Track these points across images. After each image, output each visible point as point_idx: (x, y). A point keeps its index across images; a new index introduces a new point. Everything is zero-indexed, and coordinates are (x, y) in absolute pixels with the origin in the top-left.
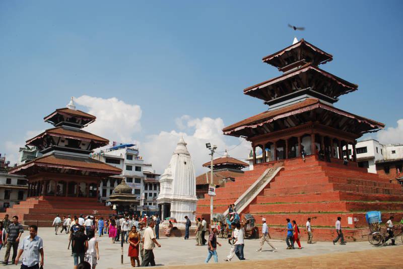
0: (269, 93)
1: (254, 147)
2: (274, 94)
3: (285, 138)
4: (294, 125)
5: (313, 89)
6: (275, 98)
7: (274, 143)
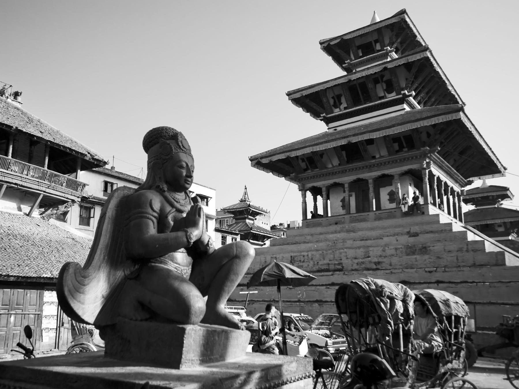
1: (303, 190)
2: (341, 104)
3: (370, 175)
6: (341, 111)
7: (346, 186)
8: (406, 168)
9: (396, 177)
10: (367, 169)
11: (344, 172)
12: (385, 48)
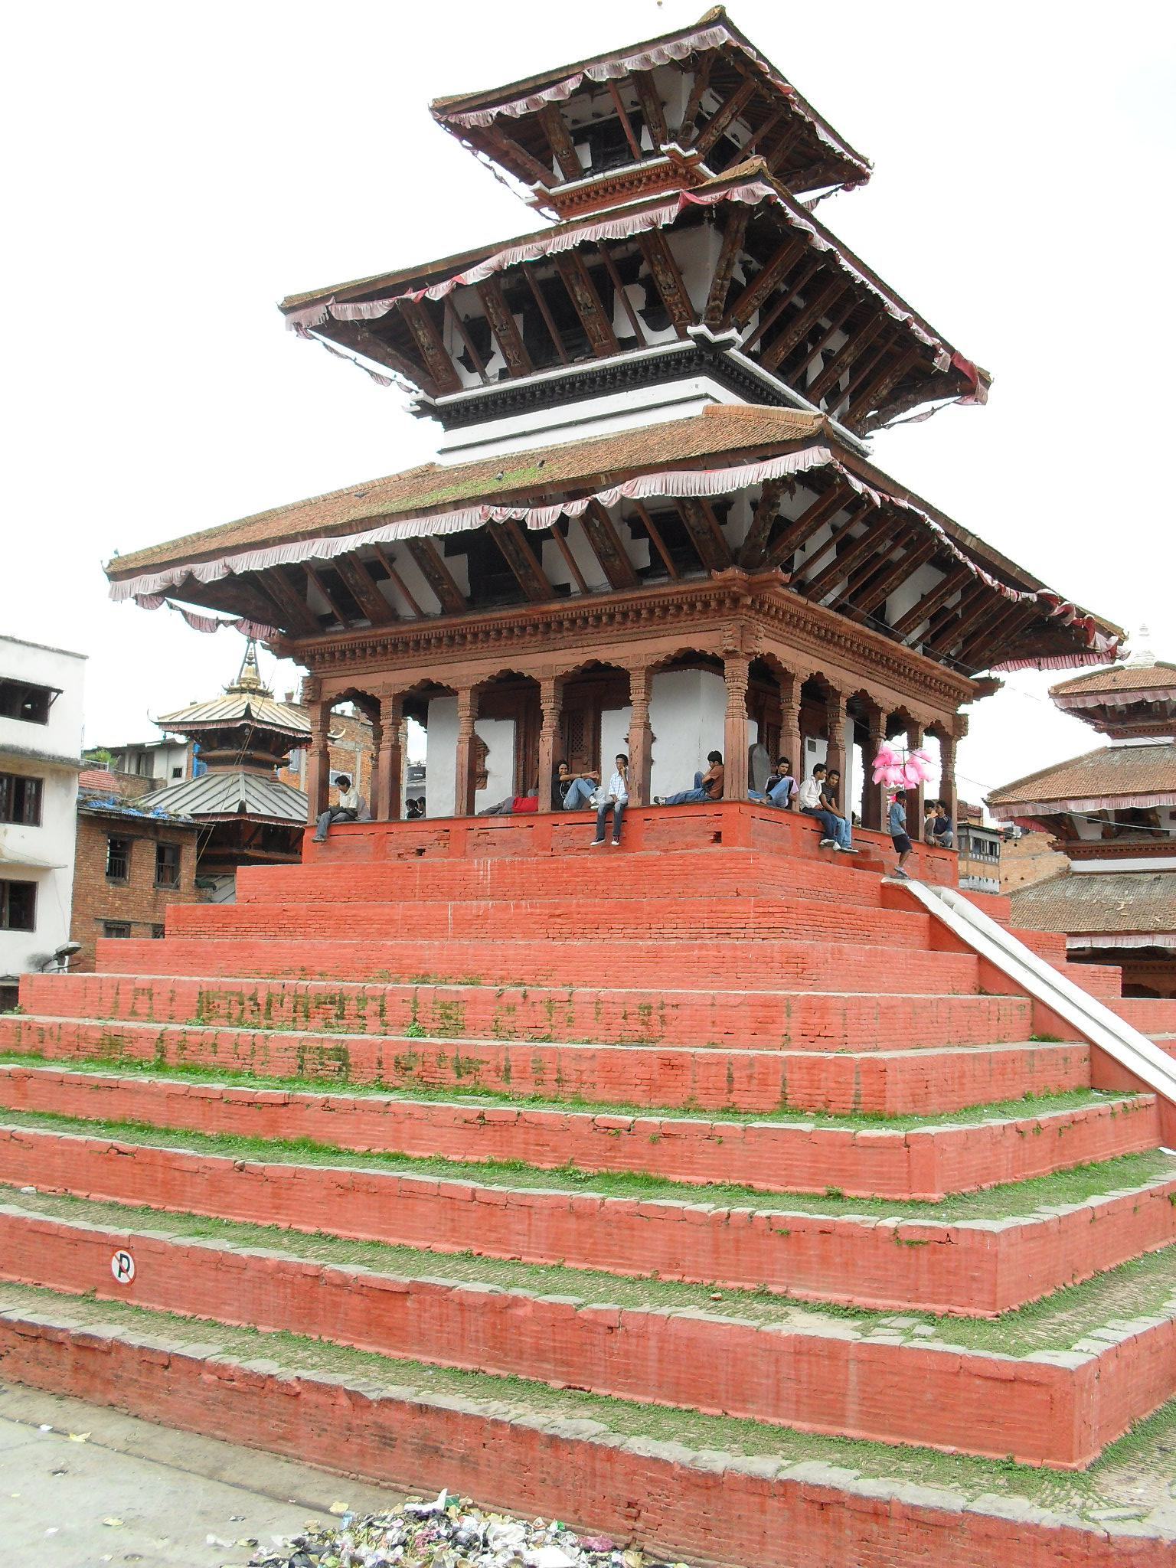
0: (456, 344)
4: (596, 576)
5: (744, 350)
6: (486, 383)
7: (465, 698)
8: (670, 645)
9: (637, 682)
10: (539, 637)
11: (455, 642)
12: (664, 148)
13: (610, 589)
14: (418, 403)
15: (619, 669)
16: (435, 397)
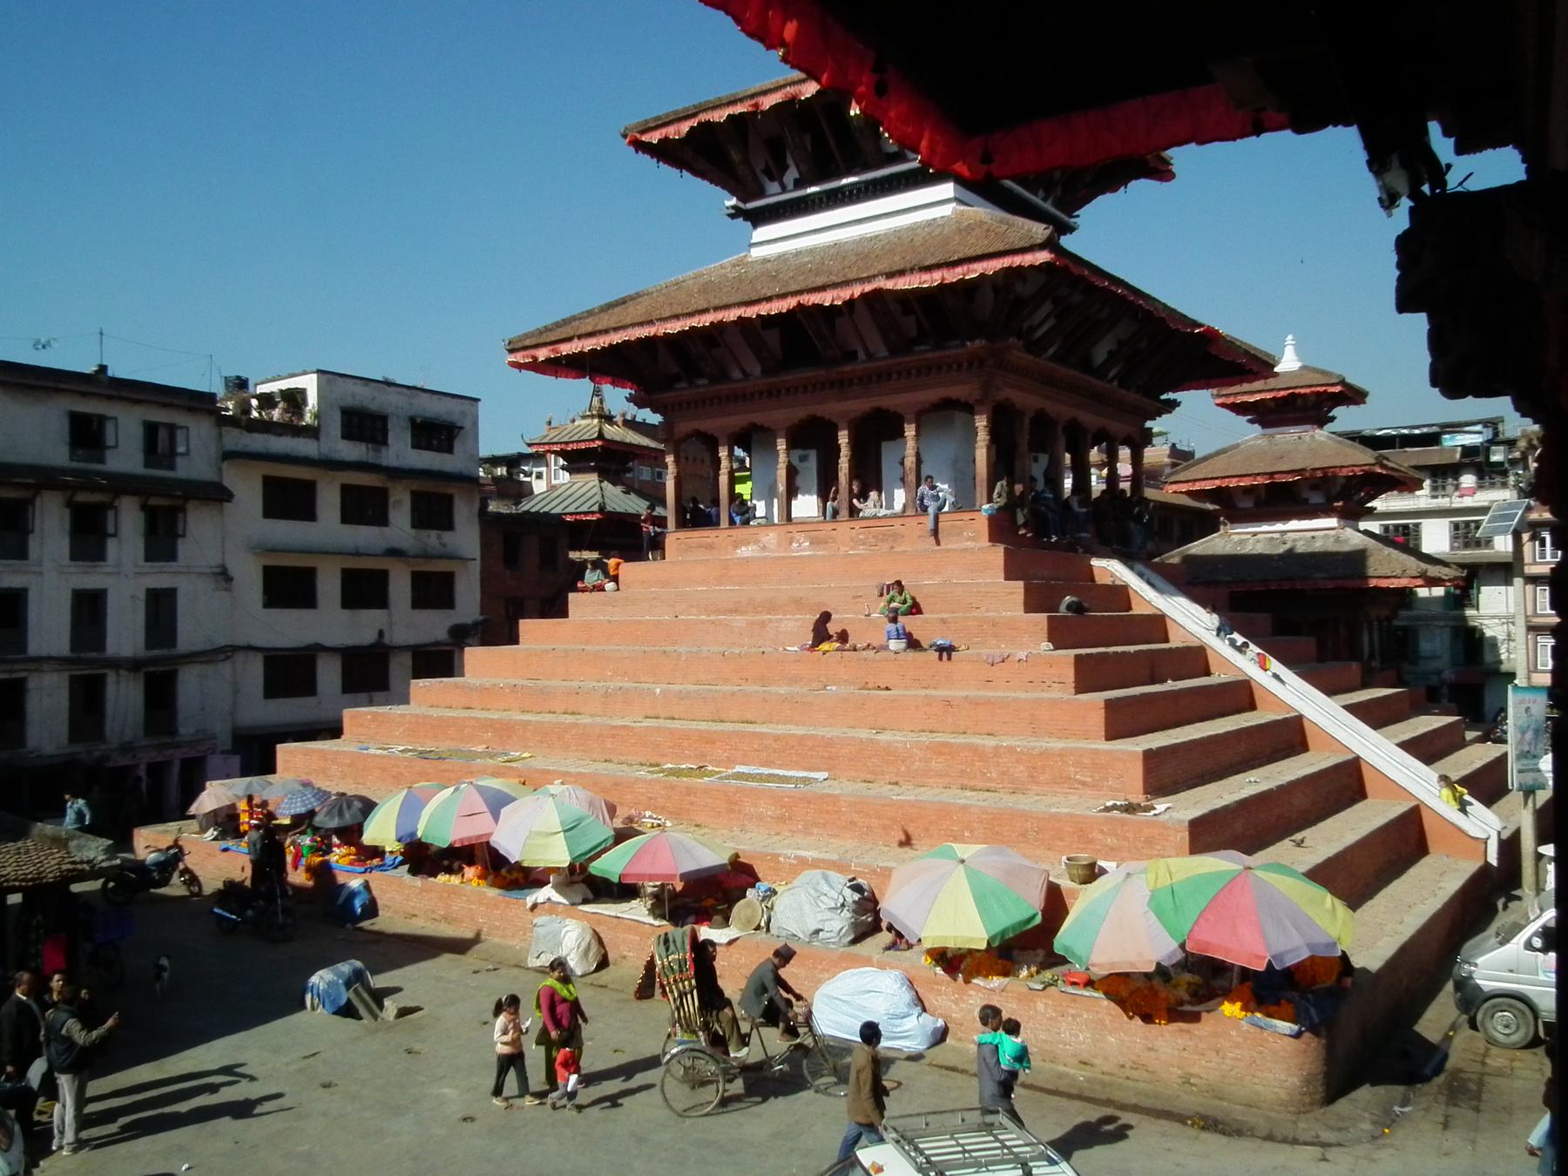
2: (785, 168)
6: (784, 189)
8: (933, 395)
11: (771, 393)
13: (886, 354)
14: (733, 207)
15: (895, 412)
16: (745, 202)
